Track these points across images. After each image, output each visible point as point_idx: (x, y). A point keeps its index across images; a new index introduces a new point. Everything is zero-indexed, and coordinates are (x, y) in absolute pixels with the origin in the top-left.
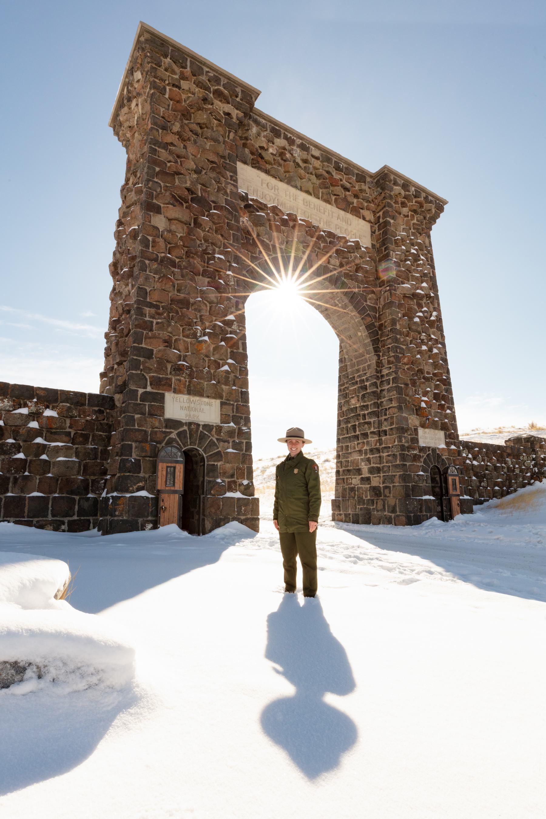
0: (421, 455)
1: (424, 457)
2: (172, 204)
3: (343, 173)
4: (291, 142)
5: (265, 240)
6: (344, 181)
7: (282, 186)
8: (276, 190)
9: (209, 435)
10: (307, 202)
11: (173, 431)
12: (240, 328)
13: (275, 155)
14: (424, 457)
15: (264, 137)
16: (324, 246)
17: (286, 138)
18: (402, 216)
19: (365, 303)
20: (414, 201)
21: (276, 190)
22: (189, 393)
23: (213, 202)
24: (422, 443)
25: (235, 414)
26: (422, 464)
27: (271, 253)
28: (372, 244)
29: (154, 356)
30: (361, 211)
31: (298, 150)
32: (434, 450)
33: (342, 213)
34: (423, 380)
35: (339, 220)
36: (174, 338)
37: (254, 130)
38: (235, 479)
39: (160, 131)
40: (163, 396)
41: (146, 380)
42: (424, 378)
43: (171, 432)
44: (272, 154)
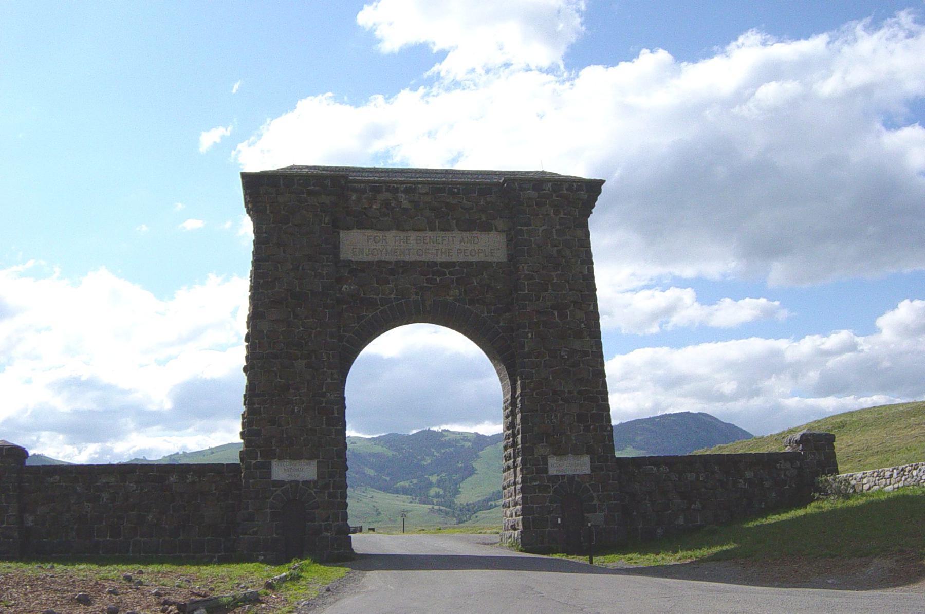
0: (551, 485)
1: (555, 486)
2: (273, 308)
3: (461, 195)
4: (396, 190)
5: (372, 296)
6: (465, 202)
7: (391, 235)
8: (384, 241)
9: (307, 488)
10: (420, 240)
11: (277, 489)
12: (335, 395)
13: (380, 208)
14: (555, 486)
15: (365, 198)
16: (440, 281)
17: (388, 190)
18: (541, 216)
19: (496, 325)
20: (554, 196)
21: (384, 241)
22: (290, 459)
23: (309, 290)
24: (552, 471)
25: (330, 470)
26: (551, 494)
27: (379, 306)
28: (509, 255)
29: (262, 434)
30: (493, 222)
31: (404, 196)
32: (571, 478)
33: (466, 235)
34: (560, 402)
35: (463, 243)
36: (277, 417)
37: (354, 197)
38: (331, 522)
39: (263, 246)
40: (270, 463)
41: (257, 453)
42: (561, 400)
43: (276, 491)
44: (375, 209)
